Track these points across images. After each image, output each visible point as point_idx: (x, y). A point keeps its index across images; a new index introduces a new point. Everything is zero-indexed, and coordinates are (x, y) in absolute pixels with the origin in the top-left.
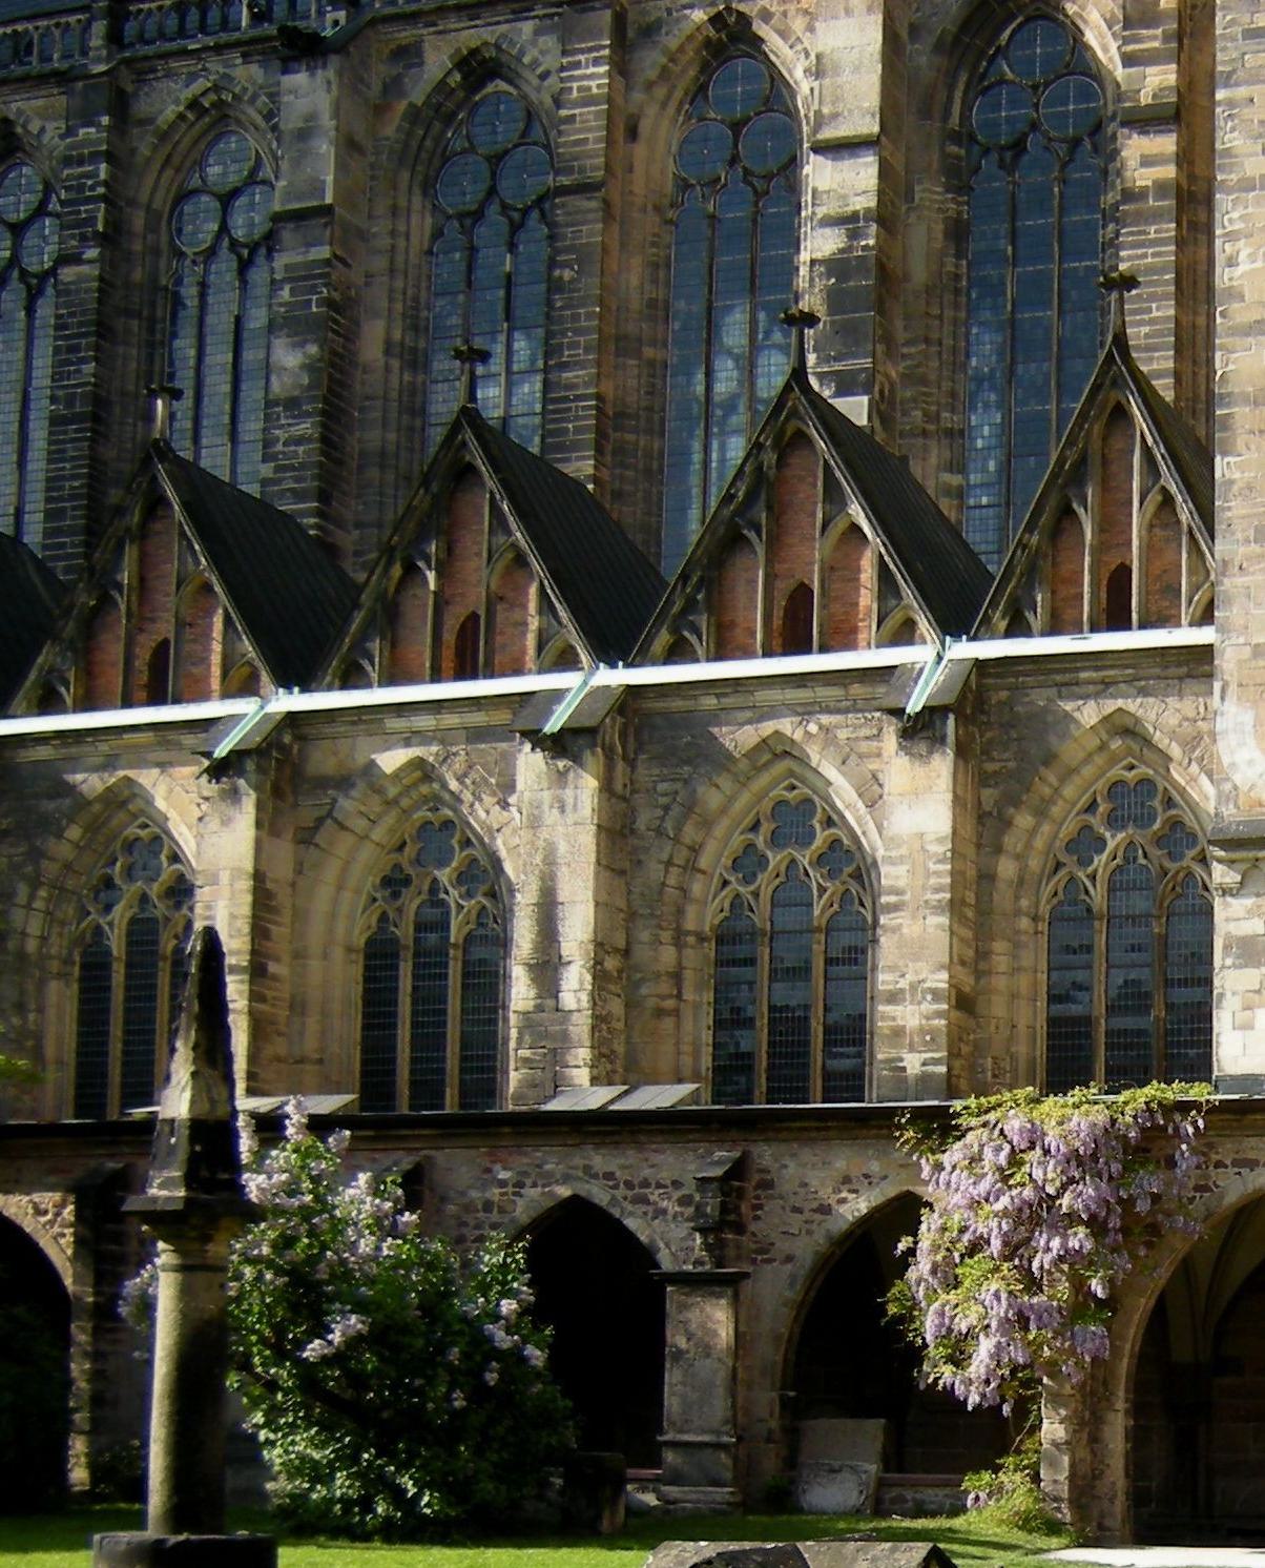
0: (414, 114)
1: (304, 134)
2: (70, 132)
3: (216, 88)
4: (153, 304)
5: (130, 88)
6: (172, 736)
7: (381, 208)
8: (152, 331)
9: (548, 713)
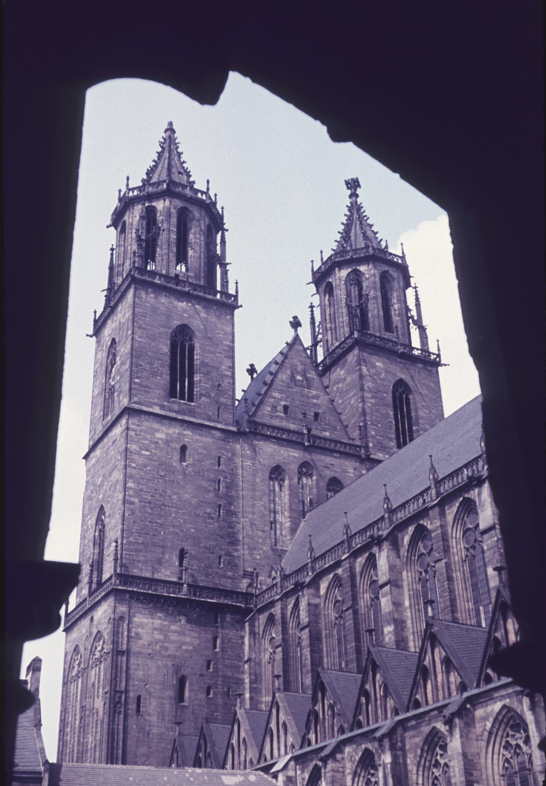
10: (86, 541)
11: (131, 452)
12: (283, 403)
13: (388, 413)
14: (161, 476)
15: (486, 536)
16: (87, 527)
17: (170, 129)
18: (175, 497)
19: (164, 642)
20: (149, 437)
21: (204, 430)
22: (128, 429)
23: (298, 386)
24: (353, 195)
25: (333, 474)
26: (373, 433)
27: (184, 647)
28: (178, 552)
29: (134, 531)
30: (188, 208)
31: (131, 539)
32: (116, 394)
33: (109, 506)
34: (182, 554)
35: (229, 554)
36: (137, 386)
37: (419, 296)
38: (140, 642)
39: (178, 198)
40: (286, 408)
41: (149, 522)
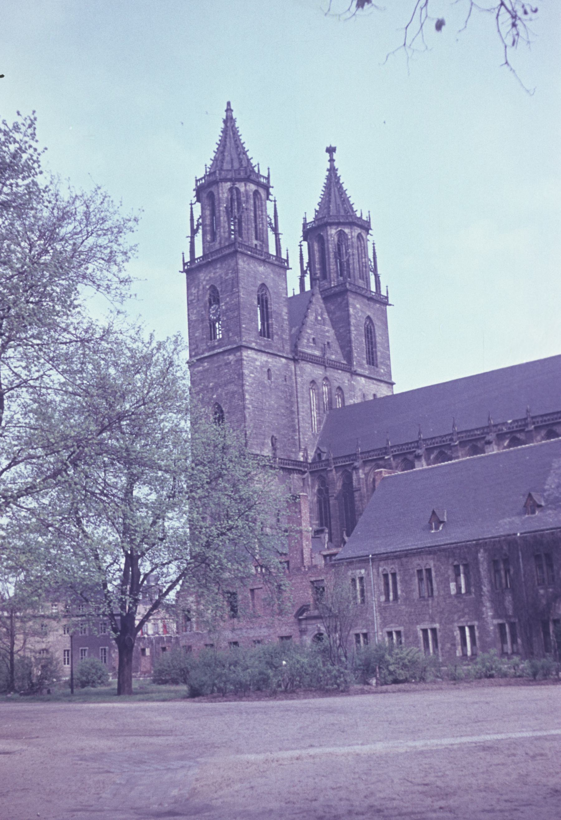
12: (313, 336)
17: (229, 110)
24: (332, 160)
37: (376, 251)
40: (314, 339)
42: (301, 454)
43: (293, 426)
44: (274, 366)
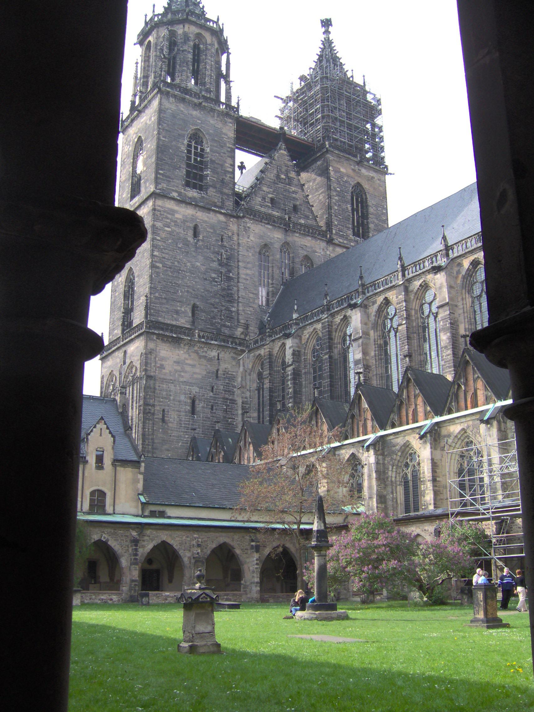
0: (464, 277)
1: (440, 288)
2: (397, 297)
3: (424, 281)
4: (418, 330)
5: (408, 285)
6: (415, 430)
7: (460, 299)
8: (419, 336)
9: (485, 415)
10: (117, 294)
11: (157, 228)
12: (270, 196)
13: (347, 208)
14: (179, 247)
15: (440, 310)
16: (118, 283)
18: (189, 264)
19: (181, 372)
20: (170, 216)
21: (211, 213)
22: (154, 209)
23: (282, 183)
25: (305, 253)
26: (336, 223)
27: (195, 376)
28: (190, 307)
29: (159, 288)
30: (201, 34)
31: (157, 295)
32: (142, 182)
33: (137, 268)
34: (194, 308)
35: (228, 309)
36: (161, 177)
38: (164, 371)
39: (194, 25)
40: (272, 200)
41: (170, 283)
42: (240, 330)
43: (230, 295)
44: (205, 222)
